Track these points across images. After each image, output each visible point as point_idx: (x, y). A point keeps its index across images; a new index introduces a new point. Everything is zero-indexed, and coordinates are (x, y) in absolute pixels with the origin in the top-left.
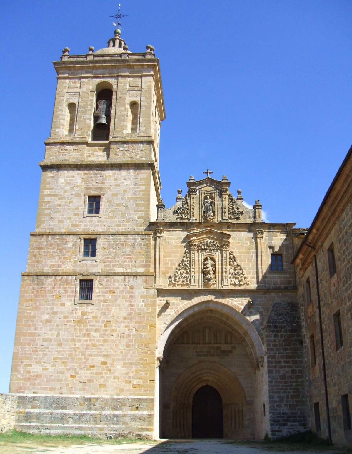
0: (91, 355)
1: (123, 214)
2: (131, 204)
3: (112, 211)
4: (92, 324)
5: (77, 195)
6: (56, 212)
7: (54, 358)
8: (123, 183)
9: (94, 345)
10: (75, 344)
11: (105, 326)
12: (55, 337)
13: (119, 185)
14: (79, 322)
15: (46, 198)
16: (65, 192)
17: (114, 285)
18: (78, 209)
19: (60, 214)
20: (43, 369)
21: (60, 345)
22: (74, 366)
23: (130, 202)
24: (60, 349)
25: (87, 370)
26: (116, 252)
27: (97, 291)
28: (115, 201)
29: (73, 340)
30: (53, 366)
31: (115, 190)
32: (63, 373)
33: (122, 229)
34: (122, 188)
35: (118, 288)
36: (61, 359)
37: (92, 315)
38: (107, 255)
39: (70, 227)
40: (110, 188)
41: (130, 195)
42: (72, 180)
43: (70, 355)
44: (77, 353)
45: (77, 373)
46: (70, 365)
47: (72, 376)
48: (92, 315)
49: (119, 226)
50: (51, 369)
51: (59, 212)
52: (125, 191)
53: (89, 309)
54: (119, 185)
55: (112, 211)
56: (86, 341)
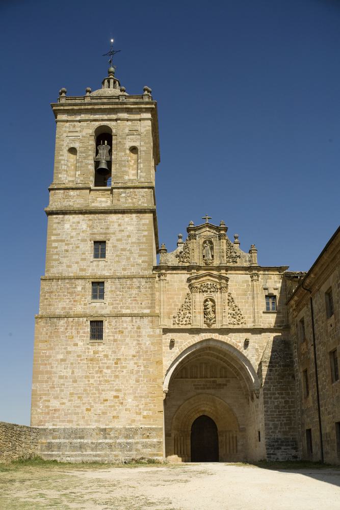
0: (103, 390)
1: (128, 259)
2: (135, 249)
3: (117, 256)
4: (103, 362)
5: (84, 240)
6: (64, 257)
7: (72, 394)
8: (127, 228)
9: (106, 381)
10: (89, 381)
11: (116, 363)
12: (70, 374)
13: (123, 231)
14: (91, 360)
15: (53, 244)
16: (72, 237)
17: (123, 325)
18: (85, 254)
19: (68, 259)
20: (61, 404)
21: (75, 381)
22: (89, 400)
23: (134, 246)
24: (75, 385)
25: (101, 403)
26: (123, 295)
27: (107, 331)
28: (120, 246)
29: (87, 377)
30: (69, 401)
31: (119, 236)
32: (78, 407)
33: (126, 273)
34: (126, 233)
35: (127, 328)
36: (77, 394)
37: (103, 353)
38: (115, 298)
39: (78, 272)
40: (114, 234)
41: (134, 240)
42: (78, 226)
43: (85, 390)
44: (92, 388)
45: (92, 406)
46: (85, 400)
47: (88, 410)
48: (103, 353)
49: (124, 269)
50: (68, 404)
51: (67, 257)
52: (129, 236)
53: (100, 348)
54: (123, 231)
55: (117, 256)
56: (99, 377)
